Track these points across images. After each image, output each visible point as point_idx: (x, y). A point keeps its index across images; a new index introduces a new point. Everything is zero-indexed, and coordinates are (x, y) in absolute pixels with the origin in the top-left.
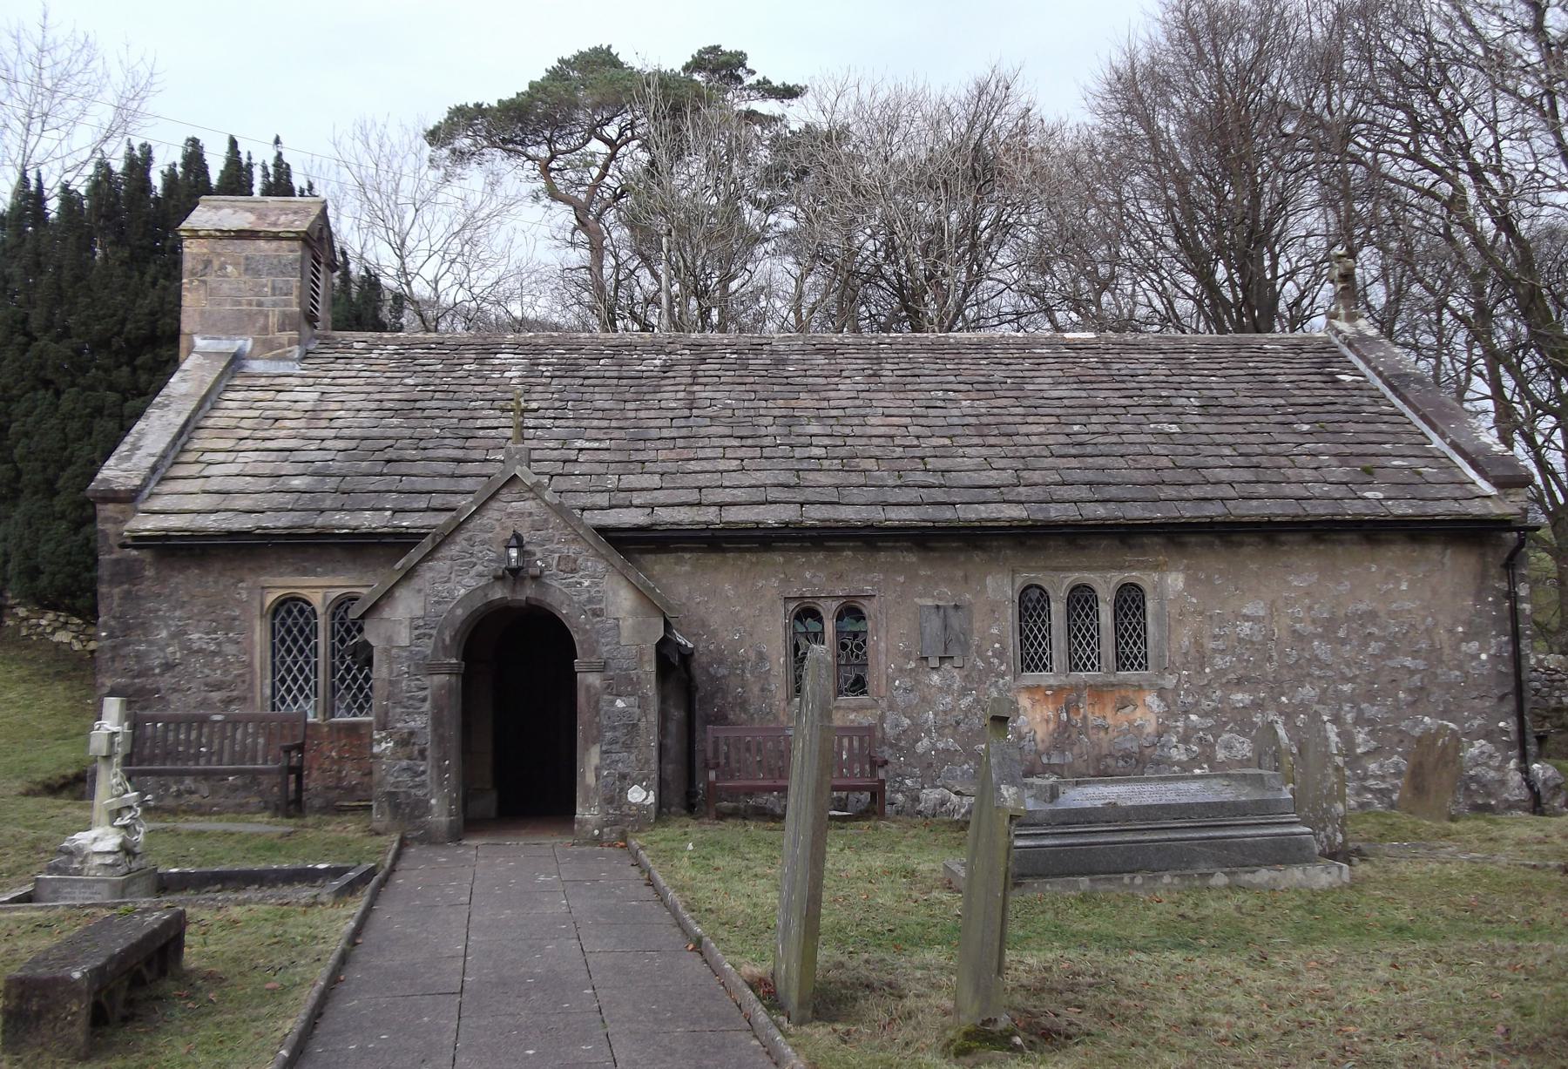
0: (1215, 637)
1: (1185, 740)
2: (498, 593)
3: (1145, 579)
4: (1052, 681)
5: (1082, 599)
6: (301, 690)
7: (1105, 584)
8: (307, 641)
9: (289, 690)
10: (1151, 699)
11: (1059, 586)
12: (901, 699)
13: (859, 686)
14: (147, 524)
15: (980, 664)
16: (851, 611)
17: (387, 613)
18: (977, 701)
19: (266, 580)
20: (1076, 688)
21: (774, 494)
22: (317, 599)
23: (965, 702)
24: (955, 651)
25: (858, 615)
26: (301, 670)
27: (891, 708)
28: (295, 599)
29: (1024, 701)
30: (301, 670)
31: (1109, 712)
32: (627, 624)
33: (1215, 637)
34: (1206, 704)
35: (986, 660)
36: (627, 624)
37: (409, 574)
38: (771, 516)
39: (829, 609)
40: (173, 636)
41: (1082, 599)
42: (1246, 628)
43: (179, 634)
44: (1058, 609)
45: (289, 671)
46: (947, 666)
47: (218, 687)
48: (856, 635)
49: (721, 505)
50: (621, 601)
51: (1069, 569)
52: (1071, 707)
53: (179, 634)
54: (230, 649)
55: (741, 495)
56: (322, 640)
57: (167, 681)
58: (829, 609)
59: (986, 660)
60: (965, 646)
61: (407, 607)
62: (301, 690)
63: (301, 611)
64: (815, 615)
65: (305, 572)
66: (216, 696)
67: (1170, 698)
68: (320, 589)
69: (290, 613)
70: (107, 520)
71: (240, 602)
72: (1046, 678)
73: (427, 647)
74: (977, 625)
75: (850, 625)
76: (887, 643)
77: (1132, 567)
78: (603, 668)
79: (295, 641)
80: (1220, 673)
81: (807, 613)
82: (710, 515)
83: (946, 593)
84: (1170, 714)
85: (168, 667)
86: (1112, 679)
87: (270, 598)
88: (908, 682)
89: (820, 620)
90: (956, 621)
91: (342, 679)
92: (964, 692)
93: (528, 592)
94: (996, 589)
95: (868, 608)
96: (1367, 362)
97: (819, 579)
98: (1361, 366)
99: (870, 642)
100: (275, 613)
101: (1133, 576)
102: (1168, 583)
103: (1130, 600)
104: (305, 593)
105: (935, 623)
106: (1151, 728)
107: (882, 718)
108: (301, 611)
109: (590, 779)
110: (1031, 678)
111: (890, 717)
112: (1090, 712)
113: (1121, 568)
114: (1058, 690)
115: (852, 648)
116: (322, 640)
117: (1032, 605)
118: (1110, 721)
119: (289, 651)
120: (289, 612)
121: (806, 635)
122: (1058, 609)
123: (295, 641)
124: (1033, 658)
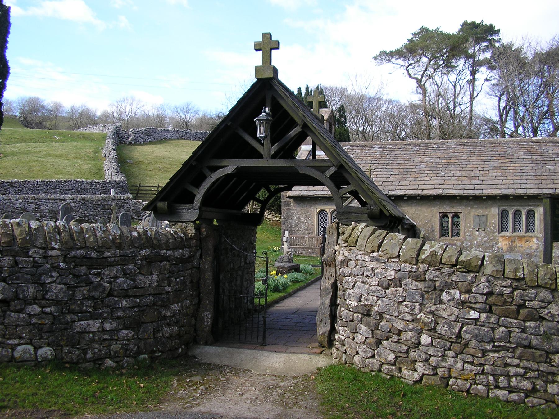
5: (517, 214)
10: (535, 240)
12: (468, 238)
13: (458, 234)
16: (456, 215)
18: (488, 239)
20: (515, 236)
22: (328, 210)
23: (484, 239)
24: (482, 226)
25: (458, 217)
27: (465, 240)
28: (323, 211)
31: (523, 243)
35: (491, 229)
39: (450, 216)
40: (297, 218)
41: (517, 214)
43: (299, 218)
46: (480, 230)
48: (457, 222)
52: (513, 242)
53: (299, 218)
54: (309, 222)
55: (429, 187)
57: (296, 228)
58: (450, 216)
60: (486, 225)
64: (448, 217)
65: (325, 205)
67: (540, 239)
72: (507, 234)
74: (488, 220)
75: (456, 219)
77: (531, 206)
82: (419, 192)
83: (480, 212)
85: (296, 225)
86: (525, 235)
88: (470, 234)
89: (448, 218)
92: (484, 237)
94: (494, 211)
95: (460, 215)
100: (319, 214)
101: (532, 208)
105: (478, 219)
106: (534, 247)
107: (463, 243)
110: (503, 234)
111: (465, 242)
112: (518, 243)
113: (528, 206)
114: (510, 237)
115: (456, 224)
117: (504, 215)
118: (523, 245)
121: (445, 221)
124: (503, 228)
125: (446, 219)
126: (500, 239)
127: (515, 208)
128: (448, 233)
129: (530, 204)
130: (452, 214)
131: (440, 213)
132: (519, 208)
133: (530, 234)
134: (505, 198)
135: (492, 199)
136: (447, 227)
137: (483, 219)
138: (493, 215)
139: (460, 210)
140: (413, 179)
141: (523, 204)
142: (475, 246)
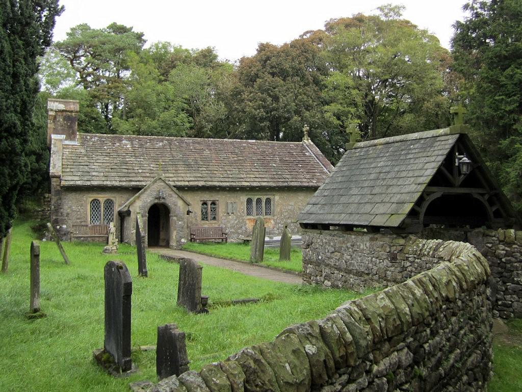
0: (284, 209)
1: (278, 229)
2: (156, 201)
3: (271, 197)
4: (253, 218)
5: (259, 201)
6: (97, 219)
7: (264, 198)
8: (98, 209)
9: (94, 220)
10: (272, 221)
11: (255, 198)
12: (223, 222)
14: (63, 183)
15: (239, 214)
16: (214, 203)
17: (134, 205)
18: (238, 221)
19: (90, 195)
21: (199, 179)
22: (101, 199)
23: (236, 222)
26: (97, 215)
28: (108, 200)
29: (247, 222)
30: (97, 215)
32: (181, 207)
33: (284, 209)
34: (282, 222)
36: (181, 207)
37: (139, 197)
38: (201, 184)
39: (209, 203)
41: (259, 201)
42: (290, 207)
44: (254, 203)
45: (94, 215)
46: (233, 214)
47: (79, 219)
49: (188, 181)
50: (180, 203)
51: (257, 195)
54: (82, 210)
56: (102, 209)
58: (209, 203)
59: (240, 213)
61: (139, 203)
62: (97, 219)
63: (97, 202)
65: (99, 194)
66: (79, 221)
68: (102, 197)
69: (95, 203)
70: (53, 182)
71: (84, 200)
73: (142, 212)
75: (213, 206)
76: (221, 209)
78: (176, 216)
79: (95, 209)
80: (285, 216)
81: (205, 203)
82: (187, 183)
83: (233, 200)
84: (276, 223)
87: (92, 199)
89: (207, 205)
90: (234, 205)
91: (106, 217)
92: (236, 220)
93: (162, 201)
94: (244, 198)
96: (311, 150)
97: (208, 197)
98: (310, 151)
99: (217, 209)
102: (277, 198)
103: (268, 201)
104: (99, 198)
108: (97, 202)
109: (174, 237)
110: (249, 217)
113: (267, 195)
115: (214, 210)
116: (102, 209)
117: (249, 201)
119: (94, 211)
120: (94, 202)
121: (204, 208)
122: (254, 203)
123: (95, 209)
125: (205, 206)
126: (247, 222)
127: (258, 197)
128: (207, 218)
129: (269, 193)
130: (211, 202)
131: (201, 201)
132: (260, 197)
133: (268, 217)
134: (252, 189)
135: (243, 189)
136: (206, 212)
137: (234, 205)
138: (242, 203)
139: (217, 199)
140: (174, 171)
141: (264, 194)
142: (229, 228)
